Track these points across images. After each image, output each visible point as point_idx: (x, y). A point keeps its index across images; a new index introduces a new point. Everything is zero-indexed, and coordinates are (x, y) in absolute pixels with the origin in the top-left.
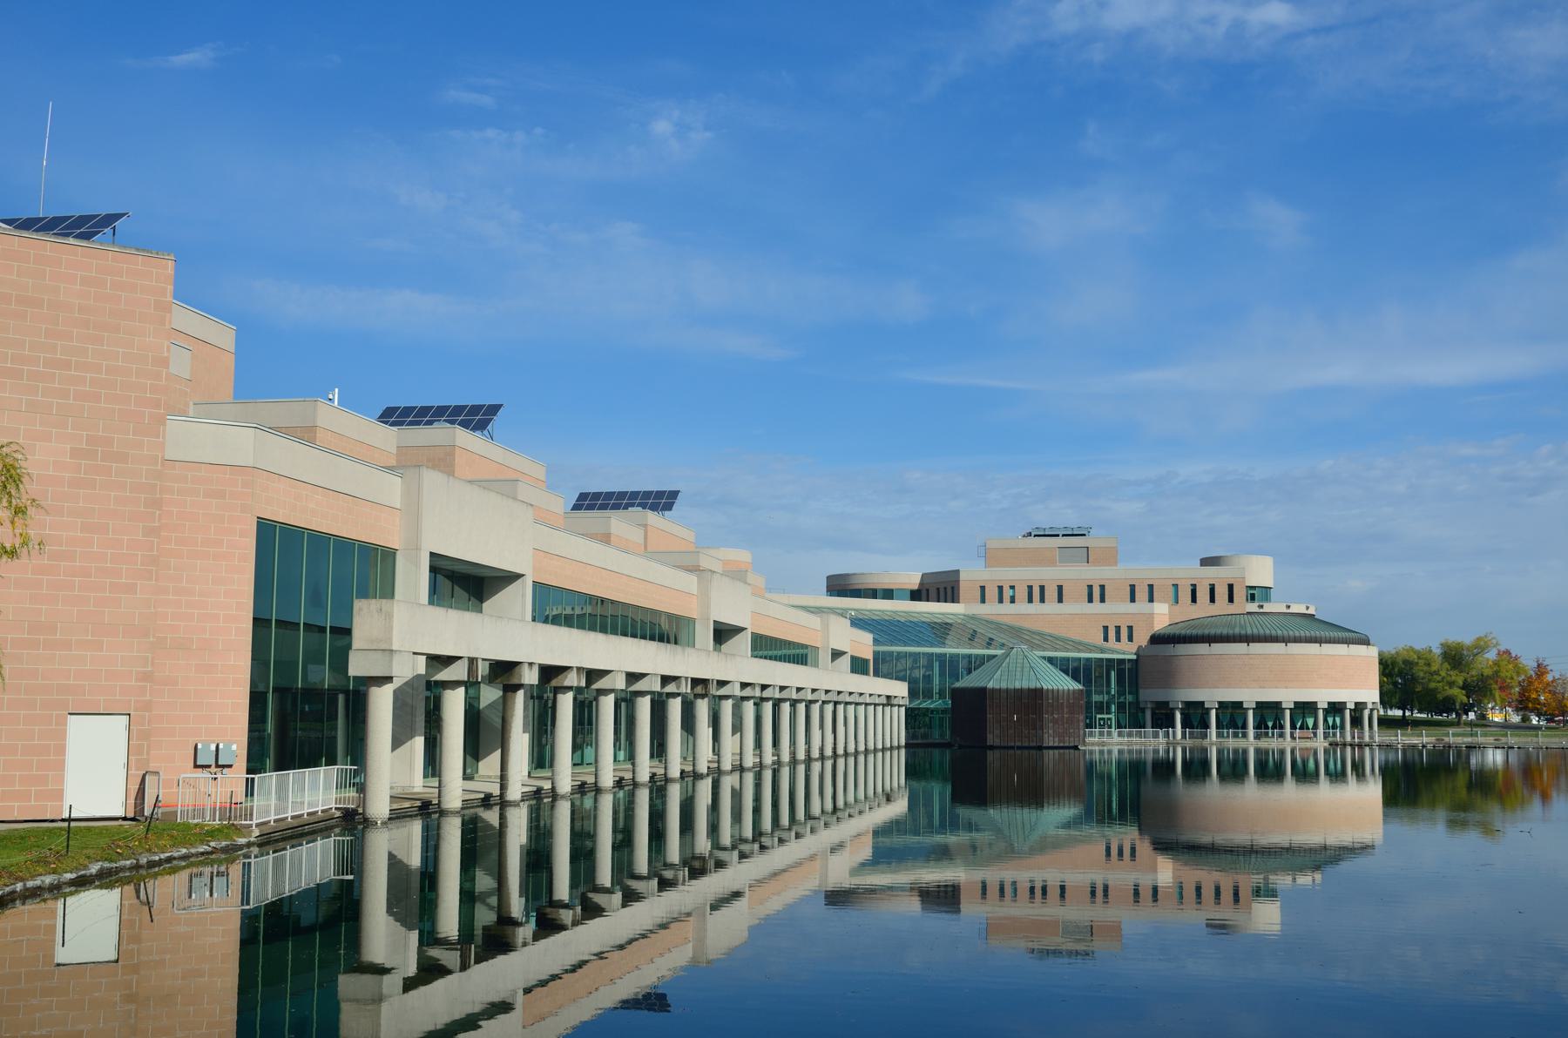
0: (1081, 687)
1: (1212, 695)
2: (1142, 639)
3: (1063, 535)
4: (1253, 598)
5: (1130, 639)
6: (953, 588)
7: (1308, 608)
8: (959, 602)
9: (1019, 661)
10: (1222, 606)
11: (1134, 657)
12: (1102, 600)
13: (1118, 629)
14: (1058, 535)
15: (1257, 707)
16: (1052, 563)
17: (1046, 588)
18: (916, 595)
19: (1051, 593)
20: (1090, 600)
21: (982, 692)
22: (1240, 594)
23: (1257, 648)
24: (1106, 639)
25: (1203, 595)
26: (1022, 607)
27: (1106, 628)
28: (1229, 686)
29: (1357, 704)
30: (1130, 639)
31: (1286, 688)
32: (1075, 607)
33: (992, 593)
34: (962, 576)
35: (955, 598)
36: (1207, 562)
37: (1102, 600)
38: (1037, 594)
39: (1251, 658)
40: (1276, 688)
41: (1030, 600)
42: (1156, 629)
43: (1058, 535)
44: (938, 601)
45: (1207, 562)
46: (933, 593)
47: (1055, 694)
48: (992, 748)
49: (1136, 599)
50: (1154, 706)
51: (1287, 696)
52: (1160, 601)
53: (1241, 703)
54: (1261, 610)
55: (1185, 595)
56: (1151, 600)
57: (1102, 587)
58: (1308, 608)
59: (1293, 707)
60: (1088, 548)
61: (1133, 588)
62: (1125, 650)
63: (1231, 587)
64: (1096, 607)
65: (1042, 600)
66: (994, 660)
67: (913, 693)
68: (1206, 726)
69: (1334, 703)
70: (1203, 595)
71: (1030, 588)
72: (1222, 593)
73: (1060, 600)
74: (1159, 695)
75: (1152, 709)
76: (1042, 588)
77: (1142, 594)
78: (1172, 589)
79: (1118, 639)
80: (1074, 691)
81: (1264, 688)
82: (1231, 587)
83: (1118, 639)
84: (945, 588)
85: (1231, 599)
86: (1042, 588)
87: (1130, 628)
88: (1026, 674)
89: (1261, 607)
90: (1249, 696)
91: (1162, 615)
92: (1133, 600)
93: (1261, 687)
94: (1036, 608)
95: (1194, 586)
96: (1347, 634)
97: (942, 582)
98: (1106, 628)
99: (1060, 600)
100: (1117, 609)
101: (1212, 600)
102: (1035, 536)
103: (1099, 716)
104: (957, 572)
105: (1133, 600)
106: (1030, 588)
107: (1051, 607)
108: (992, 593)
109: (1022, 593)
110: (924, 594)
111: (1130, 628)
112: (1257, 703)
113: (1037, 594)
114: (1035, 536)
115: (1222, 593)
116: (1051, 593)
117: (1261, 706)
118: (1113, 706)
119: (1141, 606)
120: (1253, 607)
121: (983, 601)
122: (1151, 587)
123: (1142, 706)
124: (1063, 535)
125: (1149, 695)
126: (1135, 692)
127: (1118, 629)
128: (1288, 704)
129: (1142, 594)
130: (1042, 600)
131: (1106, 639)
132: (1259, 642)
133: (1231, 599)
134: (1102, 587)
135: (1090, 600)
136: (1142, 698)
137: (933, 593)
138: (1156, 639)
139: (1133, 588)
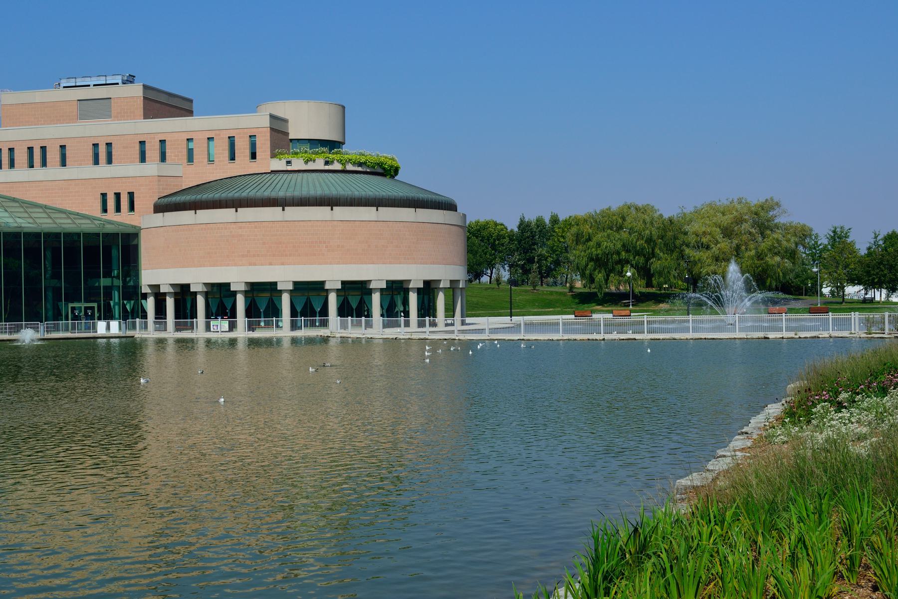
3: (94, 85)
10: (243, 165)
12: (110, 161)
13: (118, 196)
14: (89, 86)
17: (47, 149)
19: (53, 155)
20: (96, 162)
24: (105, 210)
26: (21, 174)
27: (104, 195)
29: (427, 283)
31: (283, 264)
39: (241, 228)
40: (271, 264)
43: (89, 86)
50: (178, 290)
53: (228, 285)
54: (289, 168)
59: (291, 288)
64: (103, 170)
68: (194, 315)
69: (393, 282)
71: (31, 149)
73: (63, 163)
76: (43, 149)
78: (137, 146)
79: (118, 209)
81: (255, 264)
83: (118, 209)
86: (43, 149)
87: (131, 195)
89: (289, 163)
92: (143, 159)
93: (250, 264)
94: (38, 173)
98: (104, 195)
99: (63, 163)
102: (64, 87)
103: (71, 305)
105: (143, 159)
106: (31, 149)
107: (53, 172)
109: (21, 157)
111: (131, 195)
112: (296, 283)
114: (64, 87)
116: (53, 155)
117: (300, 288)
118: (116, 292)
124: (94, 85)
127: (118, 196)
130: (44, 164)
131: (105, 210)
133: (253, 156)
135: (96, 162)
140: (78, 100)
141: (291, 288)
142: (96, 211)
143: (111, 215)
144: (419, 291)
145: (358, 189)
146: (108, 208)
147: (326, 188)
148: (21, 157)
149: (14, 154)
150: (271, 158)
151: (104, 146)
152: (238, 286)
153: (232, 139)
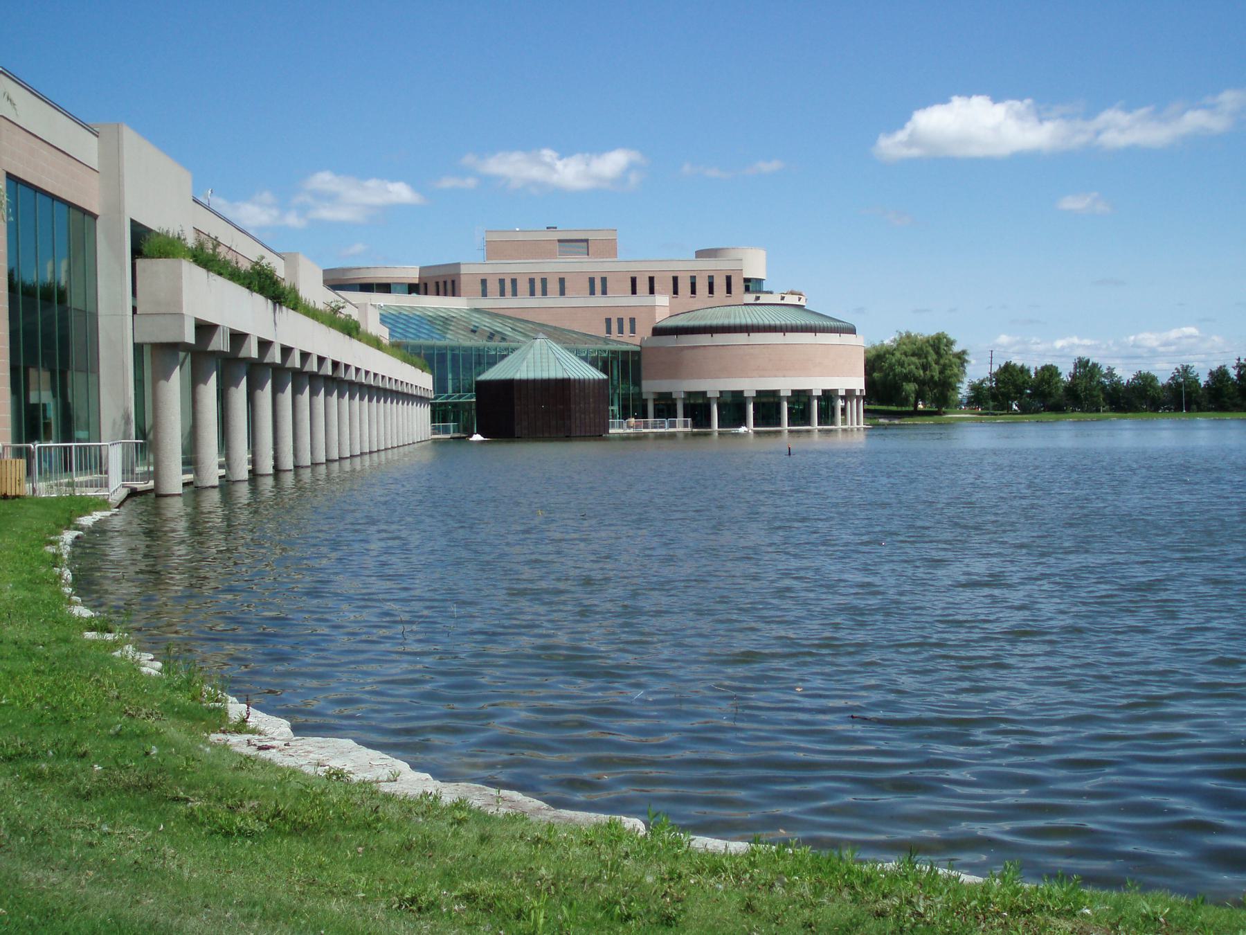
0: (605, 377)
1: (713, 386)
2: (644, 332)
4: (747, 289)
5: (633, 331)
6: (453, 282)
7: (800, 299)
8: (460, 296)
9: (544, 356)
11: (638, 349)
12: (604, 292)
13: (620, 321)
15: (757, 396)
16: (551, 255)
18: (413, 289)
19: (553, 286)
20: (592, 293)
21: (508, 386)
22: (737, 286)
23: (757, 338)
24: (609, 331)
25: (702, 287)
27: (608, 321)
28: (730, 375)
30: (633, 331)
32: (578, 299)
33: (493, 286)
34: (464, 270)
35: (456, 291)
36: (701, 254)
37: (604, 292)
38: (538, 286)
41: (532, 293)
42: (657, 320)
44: (438, 294)
45: (701, 254)
46: (432, 287)
47: (581, 384)
48: (1238, 396)
49: (637, 291)
50: (656, 397)
51: (785, 385)
52: (661, 293)
55: (684, 287)
56: (652, 291)
57: (604, 280)
58: (800, 299)
60: (587, 241)
61: (634, 281)
62: (630, 341)
63: (729, 279)
64: (599, 301)
65: (544, 293)
66: (516, 352)
67: (440, 385)
70: (702, 287)
72: (720, 284)
73: (562, 293)
74: (664, 386)
75: (654, 400)
77: (643, 286)
79: (621, 331)
80: (599, 380)
82: (729, 279)
83: (621, 331)
84: (445, 283)
85: (729, 291)
86: (544, 281)
87: (632, 321)
88: (552, 364)
90: (749, 386)
91: (662, 307)
92: (634, 292)
94: (537, 302)
95: (693, 278)
96: (832, 324)
97: (450, 275)
98: (608, 321)
99: (562, 293)
100: (619, 300)
101: (711, 291)
104: (458, 265)
105: (634, 292)
107: (554, 301)
108: (493, 286)
109: (523, 286)
110: (422, 288)
111: (632, 321)
113: (538, 286)
115: (720, 284)
116: (553, 286)
119: (642, 299)
120: (750, 298)
121: (484, 294)
122: (651, 280)
123: (644, 397)
125: (651, 387)
126: (637, 382)
127: (620, 321)
128: (786, 392)
129: (643, 286)
130: (544, 293)
131: (609, 331)
132: (759, 332)
133: (729, 291)
134: (604, 280)
135: (592, 293)
136: (644, 389)
137: (432, 287)
138: (658, 331)
139: (634, 281)
140: (560, 241)
141: (790, 394)
142: (602, 333)
143: (615, 335)
144: (819, 398)
145: (762, 317)
146: (612, 329)
147: (759, 319)
148: (523, 286)
149: (9, 261)
150: (324, 271)
151: (600, 280)
152: (713, 393)
153: (711, 278)
